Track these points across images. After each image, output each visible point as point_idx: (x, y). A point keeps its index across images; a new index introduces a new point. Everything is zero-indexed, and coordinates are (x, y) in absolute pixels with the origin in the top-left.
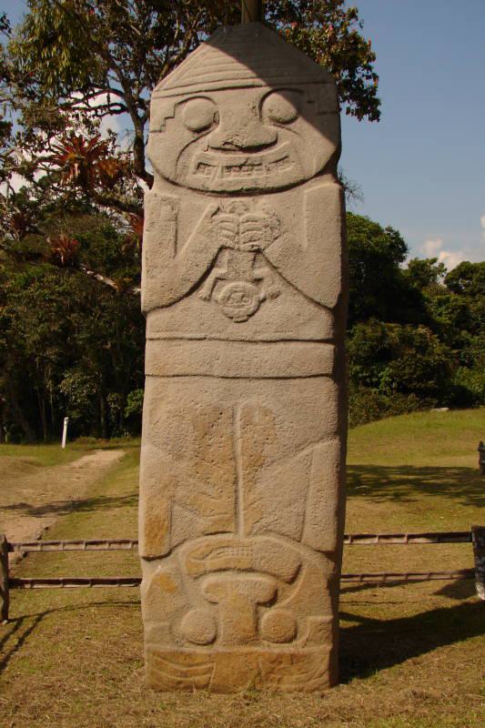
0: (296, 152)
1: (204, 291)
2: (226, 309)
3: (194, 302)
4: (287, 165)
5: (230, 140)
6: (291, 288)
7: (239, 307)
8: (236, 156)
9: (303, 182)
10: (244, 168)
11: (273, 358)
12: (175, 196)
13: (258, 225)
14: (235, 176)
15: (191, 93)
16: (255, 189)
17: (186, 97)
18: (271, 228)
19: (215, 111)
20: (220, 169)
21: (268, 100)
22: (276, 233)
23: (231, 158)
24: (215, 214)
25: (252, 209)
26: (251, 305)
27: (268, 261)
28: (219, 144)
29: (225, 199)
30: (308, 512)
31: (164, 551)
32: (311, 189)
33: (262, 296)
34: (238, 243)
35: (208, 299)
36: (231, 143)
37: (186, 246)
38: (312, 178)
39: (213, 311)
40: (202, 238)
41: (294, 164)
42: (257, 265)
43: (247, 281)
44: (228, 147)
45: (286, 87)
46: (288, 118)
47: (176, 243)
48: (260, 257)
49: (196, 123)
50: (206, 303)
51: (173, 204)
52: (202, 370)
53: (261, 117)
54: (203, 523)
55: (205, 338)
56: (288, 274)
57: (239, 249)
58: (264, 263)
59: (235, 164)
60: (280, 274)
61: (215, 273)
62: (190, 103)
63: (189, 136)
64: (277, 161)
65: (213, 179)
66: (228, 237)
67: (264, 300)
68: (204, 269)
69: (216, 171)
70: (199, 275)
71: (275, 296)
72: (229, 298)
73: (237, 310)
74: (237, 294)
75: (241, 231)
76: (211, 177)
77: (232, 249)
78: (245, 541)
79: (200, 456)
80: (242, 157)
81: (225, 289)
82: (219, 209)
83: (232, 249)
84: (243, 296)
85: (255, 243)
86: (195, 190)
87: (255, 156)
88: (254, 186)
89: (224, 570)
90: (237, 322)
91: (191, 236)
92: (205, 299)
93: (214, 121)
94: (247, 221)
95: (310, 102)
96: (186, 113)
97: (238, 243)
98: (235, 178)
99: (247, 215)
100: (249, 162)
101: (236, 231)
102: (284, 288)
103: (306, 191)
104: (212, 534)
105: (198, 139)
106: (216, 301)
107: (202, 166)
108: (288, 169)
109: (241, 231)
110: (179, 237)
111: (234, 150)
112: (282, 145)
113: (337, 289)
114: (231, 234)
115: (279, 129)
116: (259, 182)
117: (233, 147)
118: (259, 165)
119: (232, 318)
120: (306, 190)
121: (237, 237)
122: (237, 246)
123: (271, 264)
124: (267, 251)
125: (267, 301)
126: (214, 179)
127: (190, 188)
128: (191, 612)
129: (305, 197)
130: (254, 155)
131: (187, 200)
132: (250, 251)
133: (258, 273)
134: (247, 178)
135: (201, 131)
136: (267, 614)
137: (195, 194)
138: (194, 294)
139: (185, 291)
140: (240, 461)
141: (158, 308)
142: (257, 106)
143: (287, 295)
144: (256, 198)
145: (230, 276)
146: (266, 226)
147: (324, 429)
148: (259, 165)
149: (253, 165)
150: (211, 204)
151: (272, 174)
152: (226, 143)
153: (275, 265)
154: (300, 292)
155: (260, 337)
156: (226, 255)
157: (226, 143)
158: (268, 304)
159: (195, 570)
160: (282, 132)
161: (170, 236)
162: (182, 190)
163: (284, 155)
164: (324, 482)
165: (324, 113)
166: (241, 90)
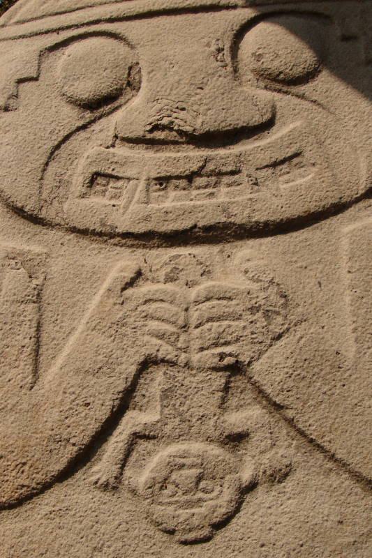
0: (321, 143)
1: (103, 466)
2: (158, 510)
4: (297, 172)
5: (165, 121)
6: (319, 456)
7: (189, 504)
8: (179, 154)
10: (199, 181)
12: (36, 248)
13: (232, 307)
14: (179, 199)
15: (77, 26)
16: (226, 226)
18: (267, 314)
19: (130, 61)
20: (142, 185)
21: (251, 37)
22: (277, 325)
23: (167, 161)
24: (131, 284)
25: (218, 270)
26: (220, 499)
27: (261, 391)
28: (139, 131)
29: (154, 252)
33: (246, 476)
34: (185, 350)
35: (112, 486)
36: (169, 127)
37: (60, 361)
39: (124, 516)
40: (101, 340)
41: (315, 169)
42: (233, 402)
43: (209, 440)
44: (160, 135)
46: (298, 71)
47: (37, 353)
48: (239, 382)
49: (86, 88)
50: (107, 496)
51: (31, 266)
53: (236, 71)
56: (311, 422)
57: (187, 365)
58: (249, 395)
59: (174, 171)
60: (290, 422)
61: (133, 421)
63: (71, 117)
64: (275, 165)
65: (126, 208)
66: (161, 336)
67: (252, 487)
68: (103, 413)
69: (137, 185)
70: (93, 427)
71: (279, 476)
73: (184, 513)
74: (185, 472)
75: (193, 321)
76: (121, 202)
77: (173, 364)
80: (192, 156)
81: (155, 460)
82: (139, 274)
83: (173, 364)
84: (200, 479)
85: (227, 349)
86: (84, 232)
88: (224, 220)
90: (185, 543)
91: (72, 339)
92: (106, 487)
93: (129, 84)
94: (208, 299)
95: (345, 38)
96: (65, 70)
97: (185, 350)
98: (179, 204)
100: (210, 167)
101: (181, 322)
102: (299, 458)
103: (347, 229)
105: (93, 121)
106: (134, 492)
107: (100, 180)
108: (300, 181)
109: (193, 321)
110: (45, 338)
111: (175, 143)
112: (285, 131)
114: (170, 328)
115: (277, 96)
116: (234, 210)
117: (173, 136)
118: (233, 173)
119: (171, 532)
121: (182, 338)
122: (183, 357)
123: (267, 397)
124: (256, 366)
125: (260, 489)
126: (128, 208)
127: (73, 230)
129: (345, 244)
130: (222, 152)
131: (65, 257)
132: (215, 369)
133: (236, 420)
134: (206, 202)
137: (84, 242)
138: (79, 475)
142: (227, 46)
144: (228, 247)
146: (253, 310)
148: (233, 173)
149: (220, 174)
150: (120, 264)
151: (264, 193)
152: (156, 128)
153: (278, 400)
154: (342, 465)
156: (157, 380)
157: (156, 128)
158: (261, 497)
160: (284, 101)
162: (53, 235)
166: (191, 17)
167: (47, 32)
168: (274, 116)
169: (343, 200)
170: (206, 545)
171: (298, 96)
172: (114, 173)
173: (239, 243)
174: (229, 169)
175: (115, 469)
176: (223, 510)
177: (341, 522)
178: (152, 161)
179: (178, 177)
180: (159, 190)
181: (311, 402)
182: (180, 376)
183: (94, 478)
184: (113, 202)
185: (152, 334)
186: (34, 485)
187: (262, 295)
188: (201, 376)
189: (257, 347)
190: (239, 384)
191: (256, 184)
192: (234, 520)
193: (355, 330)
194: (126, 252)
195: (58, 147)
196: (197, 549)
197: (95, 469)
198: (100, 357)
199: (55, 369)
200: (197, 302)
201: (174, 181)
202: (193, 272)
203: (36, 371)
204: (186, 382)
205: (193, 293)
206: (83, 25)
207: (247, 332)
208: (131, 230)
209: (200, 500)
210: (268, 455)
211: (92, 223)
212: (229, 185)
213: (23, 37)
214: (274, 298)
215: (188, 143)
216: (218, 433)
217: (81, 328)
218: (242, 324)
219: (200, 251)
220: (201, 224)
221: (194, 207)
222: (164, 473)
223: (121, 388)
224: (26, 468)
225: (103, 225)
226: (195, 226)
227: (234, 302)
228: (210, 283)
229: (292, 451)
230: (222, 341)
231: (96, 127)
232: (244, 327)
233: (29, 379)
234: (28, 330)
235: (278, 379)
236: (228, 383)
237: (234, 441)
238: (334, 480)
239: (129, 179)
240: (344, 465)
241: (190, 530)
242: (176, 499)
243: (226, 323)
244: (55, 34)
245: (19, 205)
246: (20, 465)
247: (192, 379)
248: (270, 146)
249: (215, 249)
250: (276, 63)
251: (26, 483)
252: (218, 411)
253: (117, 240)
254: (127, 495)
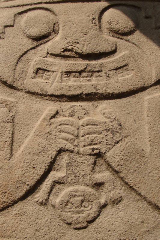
0: (136, 61)
1: (40, 194)
2: (64, 215)
3: (29, 206)
4: (125, 72)
5: (70, 48)
6: (134, 194)
7: (78, 212)
8: (75, 62)
12: (12, 99)
14: (75, 81)
15: (31, 4)
16: (96, 94)
18: (113, 132)
19: (55, 21)
20: (59, 74)
21: (107, 14)
22: (117, 137)
23: (70, 64)
24: (54, 117)
25: (91, 113)
26: (91, 211)
27: (109, 165)
28: (58, 51)
29: (64, 104)
32: (151, 96)
33: (103, 201)
34: (77, 146)
35: (44, 204)
36: (71, 50)
37: (22, 148)
38: (151, 86)
39: (49, 216)
40: (40, 140)
41: (133, 72)
42: (97, 169)
43: (87, 185)
46: (127, 30)
47: (12, 144)
48: (100, 161)
49: (35, 31)
50: (42, 208)
51: (10, 107)
53: (100, 28)
56: (131, 179)
57: (78, 153)
58: (104, 167)
60: (122, 179)
61: (53, 176)
63: (28, 43)
64: (116, 69)
65: (52, 84)
66: (67, 140)
67: (105, 206)
68: (41, 172)
69: (57, 74)
70: (36, 178)
71: (116, 202)
73: (75, 216)
74: (76, 198)
75: (81, 134)
76: (50, 81)
80: (81, 64)
81: (63, 193)
82: (57, 113)
84: (83, 201)
85: (96, 147)
86: (33, 93)
87: (95, 64)
88: (94, 91)
90: (76, 229)
91: (28, 139)
92: (41, 203)
93: (54, 31)
94: (87, 125)
95: (147, 17)
96: (26, 23)
98: (75, 83)
99: (86, 119)
101: (76, 134)
102: (125, 194)
103: (146, 98)
106: (54, 206)
107: (40, 71)
108: (127, 77)
109: (81, 134)
110: (15, 138)
111: (74, 57)
112: (121, 55)
115: (118, 40)
116: (99, 87)
117: (73, 54)
118: (99, 71)
119: (70, 224)
121: (76, 141)
123: (112, 168)
124: (108, 154)
126: (53, 84)
127: (28, 92)
129: (146, 104)
130: (94, 62)
131: (24, 104)
132: (90, 155)
133: (99, 177)
134: (87, 83)
137: (33, 98)
138: (29, 198)
142: (97, 17)
143: (129, 199)
144: (96, 103)
145: (69, 180)
146: (107, 130)
148: (99, 71)
149: (93, 72)
150: (49, 108)
151: (112, 81)
152: (66, 50)
153: (117, 169)
154: (144, 198)
156: (65, 158)
157: (66, 50)
158: (109, 210)
160: (120, 42)
162: (19, 94)
163: (123, 64)
167: (18, 6)
168: (116, 48)
169: (145, 86)
170: (85, 230)
171: (126, 41)
172: (47, 69)
173: (101, 102)
174: (97, 70)
175: (46, 196)
176: (93, 215)
177: (143, 222)
179: (75, 72)
180: (67, 77)
181: (131, 171)
182: (75, 157)
183: (36, 200)
184: (46, 81)
185: (63, 139)
186: (10, 202)
187: (111, 124)
188: (84, 158)
189: (108, 146)
190: (100, 161)
191: (108, 77)
192: (97, 220)
193: (150, 141)
194: (52, 103)
195: (22, 56)
196: (81, 231)
197: (37, 196)
198: (40, 148)
199: (20, 152)
200: (83, 126)
201: (73, 73)
202: (81, 113)
203: (11, 152)
204: (77, 160)
205: (81, 122)
206: (34, 4)
207: (104, 139)
208: (54, 94)
209: (82, 211)
210: (112, 193)
211: (37, 90)
212: (97, 77)
213: (7, 7)
214: (116, 126)
215: (79, 58)
216: (91, 182)
217: (31, 135)
218: (102, 136)
219: (84, 104)
220: (84, 93)
221: (82, 85)
222: (67, 199)
223: (49, 161)
224: (7, 194)
225: (42, 91)
226: (82, 93)
227: (99, 127)
228: (88, 118)
229: (122, 191)
230: (93, 143)
231: (39, 48)
232: (103, 138)
233: (9, 156)
234: (8, 134)
235: (117, 160)
236: (95, 161)
237: (97, 186)
238: (140, 204)
239: (53, 72)
240: (144, 198)
241: (78, 223)
242: (72, 210)
243: (95, 135)
244: (21, 7)
245: (5, 80)
246: (4, 193)
247: (80, 159)
248: (114, 61)
249: (91, 103)
250: (118, 26)
251: (6, 201)
252: (91, 173)
253: (47, 98)
254: (50, 207)
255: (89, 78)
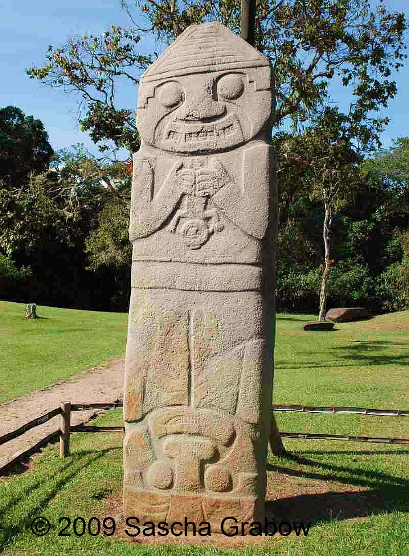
5: (191, 114)
7: (195, 238)
9: (243, 143)
10: (201, 134)
11: (217, 276)
13: (208, 177)
14: (194, 140)
16: (208, 150)
17: (162, 81)
30: (240, 393)
31: (139, 416)
42: (208, 207)
44: (189, 118)
45: (237, 70)
49: (170, 100)
52: (168, 284)
54: (166, 397)
55: (171, 261)
59: (193, 131)
61: (179, 213)
62: (166, 85)
63: (164, 111)
67: (213, 233)
68: (170, 210)
70: (167, 214)
72: (187, 231)
73: (193, 240)
78: (194, 413)
79: (165, 347)
80: (200, 125)
82: (182, 166)
84: (197, 231)
85: (206, 191)
87: (208, 125)
89: (180, 433)
95: (250, 82)
104: (172, 406)
105: (170, 113)
113: (264, 225)
115: (227, 104)
118: (211, 131)
120: (244, 150)
126: (179, 143)
128: (157, 462)
133: (209, 213)
135: (174, 106)
136: (210, 468)
137: (167, 154)
139: (158, 226)
140: (193, 353)
141: (139, 238)
147: (252, 330)
152: (188, 116)
155: (208, 261)
156: (186, 198)
159: (160, 432)
161: (148, 186)
164: (253, 371)
165: (260, 90)
166: (200, 75)
174: (210, 130)
178: (185, 128)
195: (159, 122)
199: (157, 196)
202: (197, 165)
217: (165, 183)
223: (176, 202)
226: (199, 150)
232: (212, 184)
249: (205, 157)
255: (205, 137)
